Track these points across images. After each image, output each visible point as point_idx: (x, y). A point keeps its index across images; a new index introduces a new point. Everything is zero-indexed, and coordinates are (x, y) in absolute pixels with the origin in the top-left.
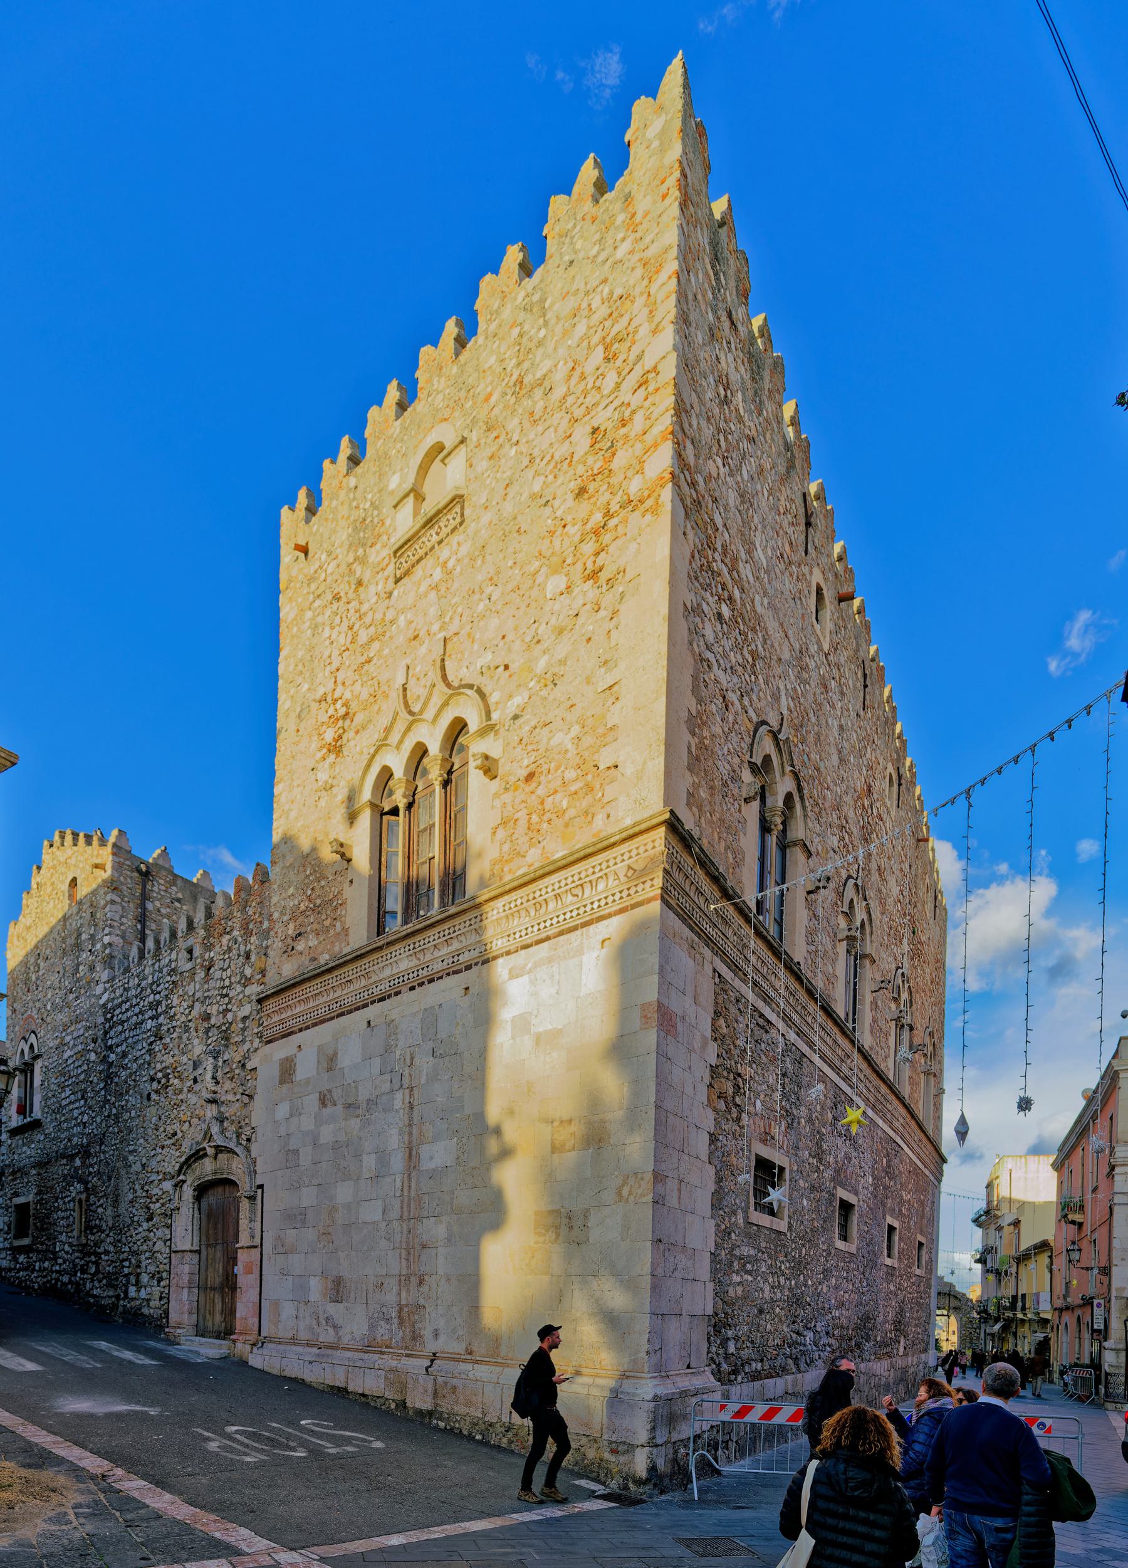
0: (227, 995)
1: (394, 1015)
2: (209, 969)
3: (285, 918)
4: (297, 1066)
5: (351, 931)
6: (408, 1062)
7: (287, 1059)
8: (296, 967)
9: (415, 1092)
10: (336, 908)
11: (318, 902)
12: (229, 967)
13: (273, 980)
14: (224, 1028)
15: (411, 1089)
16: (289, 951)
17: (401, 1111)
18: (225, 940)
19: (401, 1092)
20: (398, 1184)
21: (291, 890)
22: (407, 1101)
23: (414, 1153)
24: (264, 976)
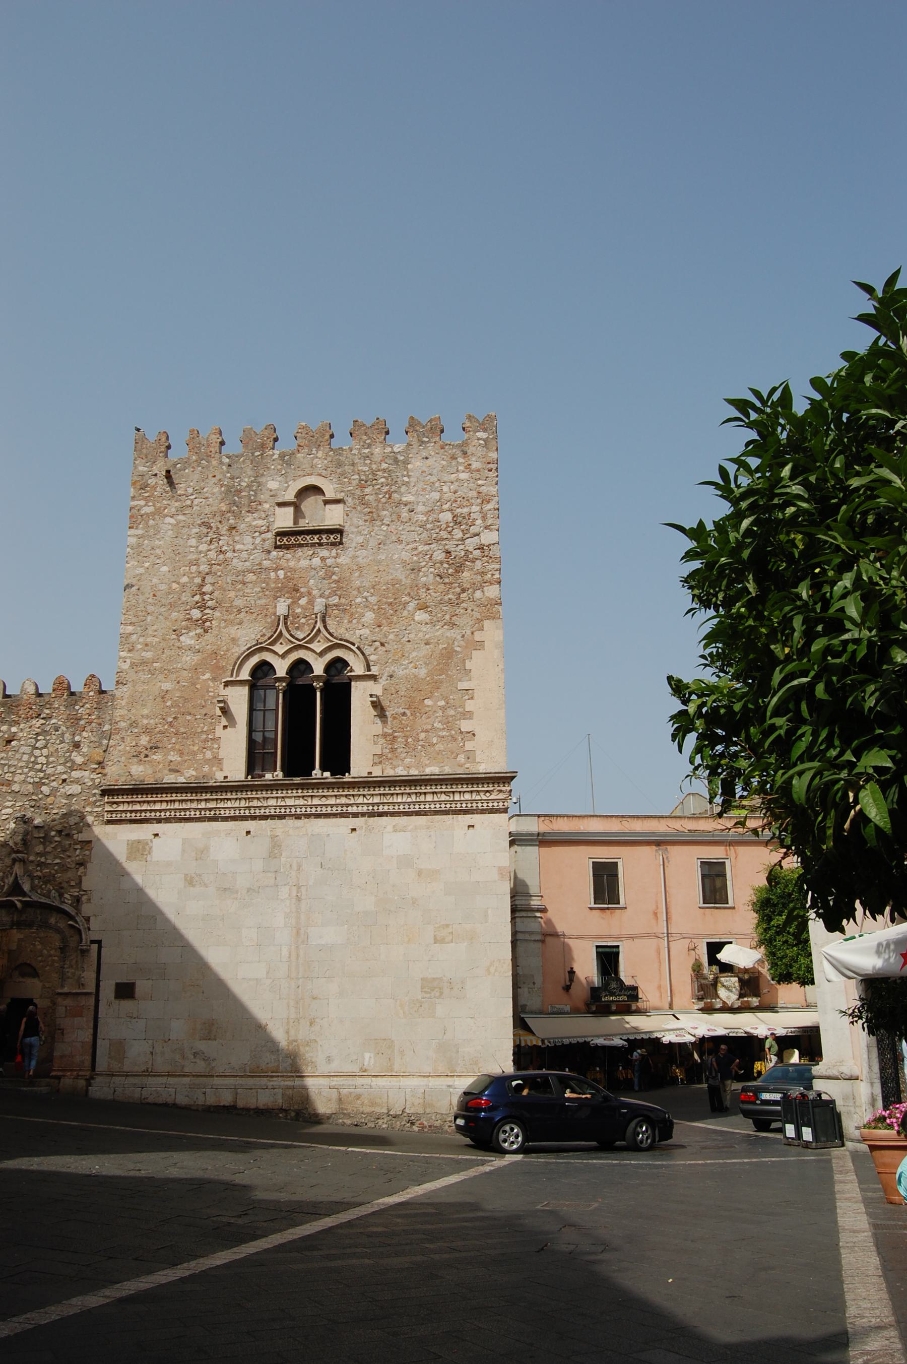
0: (41, 771)
1: (279, 832)
2: (9, 742)
3: (136, 730)
4: (154, 849)
5: (225, 762)
6: (295, 867)
7: (139, 842)
8: (150, 771)
9: (303, 889)
10: (206, 740)
11: (182, 730)
12: (45, 747)
13: (115, 774)
14: (34, 797)
15: (299, 888)
16: (140, 756)
17: (288, 902)
18: (37, 723)
19: (287, 888)
20: (285, 952)
21: (146, 712)
22: (294, 893)
23: (302, 931)
24: (103, 768)
